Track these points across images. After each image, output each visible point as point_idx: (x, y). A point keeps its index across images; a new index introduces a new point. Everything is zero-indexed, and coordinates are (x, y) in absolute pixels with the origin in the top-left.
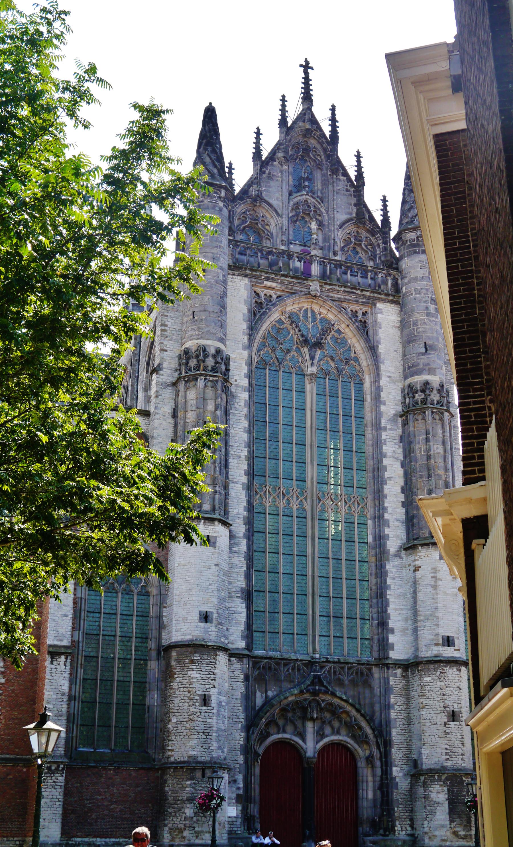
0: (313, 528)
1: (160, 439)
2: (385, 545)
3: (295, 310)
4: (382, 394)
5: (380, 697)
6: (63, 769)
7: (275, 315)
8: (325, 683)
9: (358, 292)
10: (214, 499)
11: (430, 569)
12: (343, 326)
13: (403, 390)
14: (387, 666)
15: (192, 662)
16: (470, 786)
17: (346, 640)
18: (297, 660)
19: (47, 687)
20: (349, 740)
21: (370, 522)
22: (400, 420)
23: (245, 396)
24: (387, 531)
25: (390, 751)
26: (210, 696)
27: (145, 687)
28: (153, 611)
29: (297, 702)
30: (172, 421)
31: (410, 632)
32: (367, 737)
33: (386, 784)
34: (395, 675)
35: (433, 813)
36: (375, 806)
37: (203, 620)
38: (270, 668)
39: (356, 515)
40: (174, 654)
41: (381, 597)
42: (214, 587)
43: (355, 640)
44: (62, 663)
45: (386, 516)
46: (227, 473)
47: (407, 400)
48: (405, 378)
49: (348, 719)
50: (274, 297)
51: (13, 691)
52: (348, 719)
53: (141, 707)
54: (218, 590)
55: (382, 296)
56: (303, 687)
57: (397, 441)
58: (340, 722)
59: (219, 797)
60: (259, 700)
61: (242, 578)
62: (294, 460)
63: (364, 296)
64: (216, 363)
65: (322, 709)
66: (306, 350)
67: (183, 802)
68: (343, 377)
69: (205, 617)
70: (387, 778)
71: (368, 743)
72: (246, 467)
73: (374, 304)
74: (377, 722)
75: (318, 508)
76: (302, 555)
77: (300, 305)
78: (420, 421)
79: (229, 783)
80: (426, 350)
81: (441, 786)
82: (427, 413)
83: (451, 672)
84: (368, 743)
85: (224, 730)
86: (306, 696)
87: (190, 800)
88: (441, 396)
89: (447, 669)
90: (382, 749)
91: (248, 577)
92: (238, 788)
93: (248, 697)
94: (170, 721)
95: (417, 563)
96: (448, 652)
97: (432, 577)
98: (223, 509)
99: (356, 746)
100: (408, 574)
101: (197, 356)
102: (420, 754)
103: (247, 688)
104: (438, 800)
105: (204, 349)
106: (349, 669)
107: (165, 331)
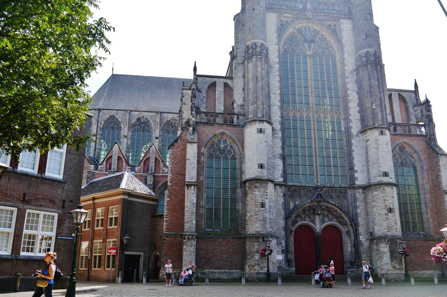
0: (314, 125)
1: (237, 88)
3: (300, 27)
4: (345, 61)
5: (352, 203)
6: (195, 238)
7: (291, 30)
8: (324, 197)
9: (331, 15)
10: (263, 112)
12: (324, 32)
13: (356, 59)
14: (355, 188)
15: (256, 187)
16: (401, 244)
17: (333, 177)
18: (309, 187)
19: (186, 200)
20: (337, 224)
21: (342, 122)
22: (355, 73)
23: (278, 66)
24: (351, 125)
25: (358, 228)
26: (265, 203)
27: (236, 201)
28: (238, 166)
29: (310, 206)
30: (243, 80)
31: (365, 171)
32: (346, 222)
33: (357, 245)
34: (359, 192)
35: (382, 257)
36: (352, 255)
37: (260, 167)
38: (296, 191)
39: (335, 118)
40: (247, 184)
41: (350, 156)
42: (265, 152)
43: (337, 177)
44: (193, 189)
45: (350, 118)
46: (270, 100)
47: (358, 62)
48: (357, 52)
49: (336, 214)
50: (290, 21)
51: (173, 204)
52: (336, 214)
53: (234, 210)
54: (267, 153)
55: (343, 16)
56: (313, 199)
58: (333, 215)
59: (269, 250)
60: (292, 206)
61: (280, 149)
62: (303, 95)
63: (334, 17)
64: (261, 50)
65: (323, 210)
66: (306, 44)
67: (254, 253)
68: (325, 56)
69: (261, 166)
70: (357, 241)
71: (346, 225)
72: (279, 98)
73: (339, 20)
74: (351, 215)
75: (316, 116)
76: (310, 138)
77: (303, 24)
79: (277, 244)
80: (366, 37)
81: (385, 244)
83: (388, 189)
84: (346, 225)
85: (274, 219)
86: (315, 203)
87: (257, 252)
88: (376, 58)
89: (386, 188)
90: (354, 228)
91: (283, 148)
92: (283, 247)
93: (286, 205)
94: (247, 215)
95: (367, 138)
96: (386, 180)
98: (268, 116)
99: (341, 227)
100: (363, 144)
101: (252, 47)
102: (374, 229)
103: (285, 200)
104: (384, 251)
105: (255, 44)
106: (336, 190)
107: (238, 40)
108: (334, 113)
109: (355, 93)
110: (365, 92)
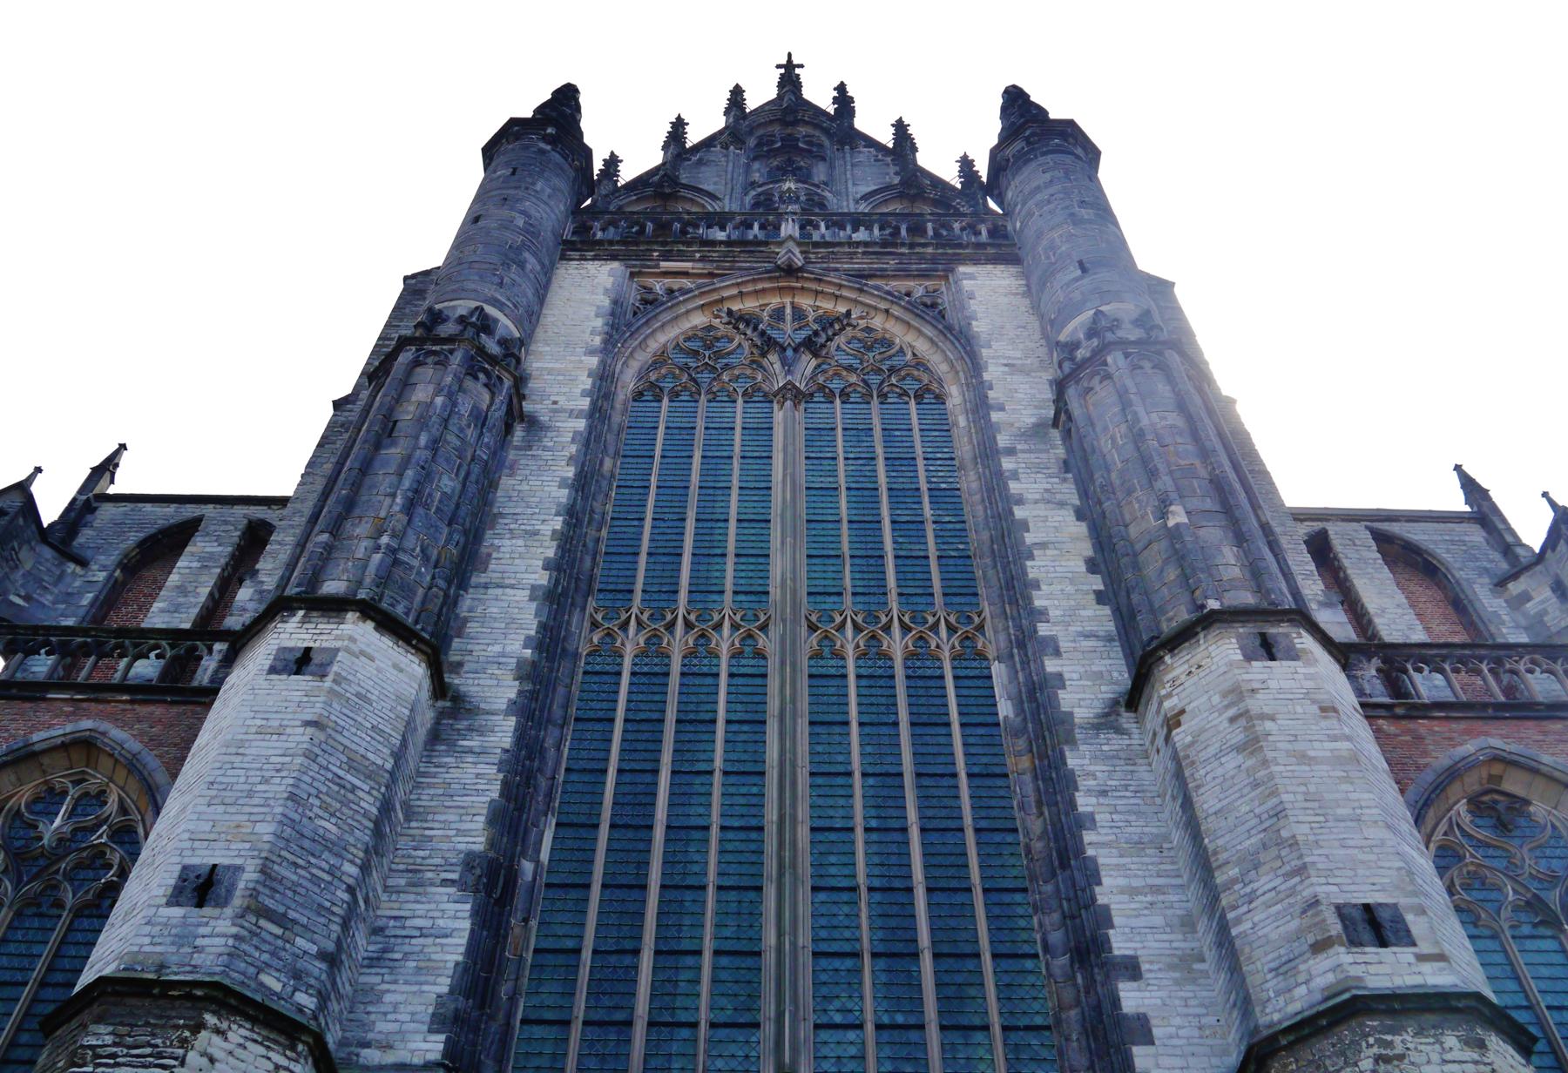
2: (1053, 701)
11: (1216, 699)
21: (998, 671)
22: (1055, 434)
24: (1051, 665)
39: (946, 654)
41: (1064, 865)
42: (279, 787)
54: (292, 797)
57: (1054, 470)
73: (952, 270)
78: (1098, 388)
80: (1084, 270)
82: (1109, 360)
96: (1386, 970)
97: (1232, 720)
100: (1154, 773)
108: (936, 625)
109: (1068, 516)
110: (1114, 475)
